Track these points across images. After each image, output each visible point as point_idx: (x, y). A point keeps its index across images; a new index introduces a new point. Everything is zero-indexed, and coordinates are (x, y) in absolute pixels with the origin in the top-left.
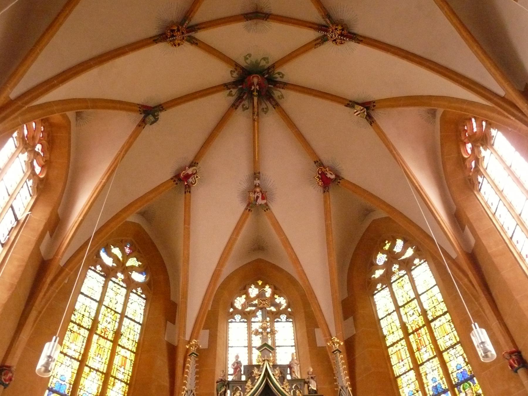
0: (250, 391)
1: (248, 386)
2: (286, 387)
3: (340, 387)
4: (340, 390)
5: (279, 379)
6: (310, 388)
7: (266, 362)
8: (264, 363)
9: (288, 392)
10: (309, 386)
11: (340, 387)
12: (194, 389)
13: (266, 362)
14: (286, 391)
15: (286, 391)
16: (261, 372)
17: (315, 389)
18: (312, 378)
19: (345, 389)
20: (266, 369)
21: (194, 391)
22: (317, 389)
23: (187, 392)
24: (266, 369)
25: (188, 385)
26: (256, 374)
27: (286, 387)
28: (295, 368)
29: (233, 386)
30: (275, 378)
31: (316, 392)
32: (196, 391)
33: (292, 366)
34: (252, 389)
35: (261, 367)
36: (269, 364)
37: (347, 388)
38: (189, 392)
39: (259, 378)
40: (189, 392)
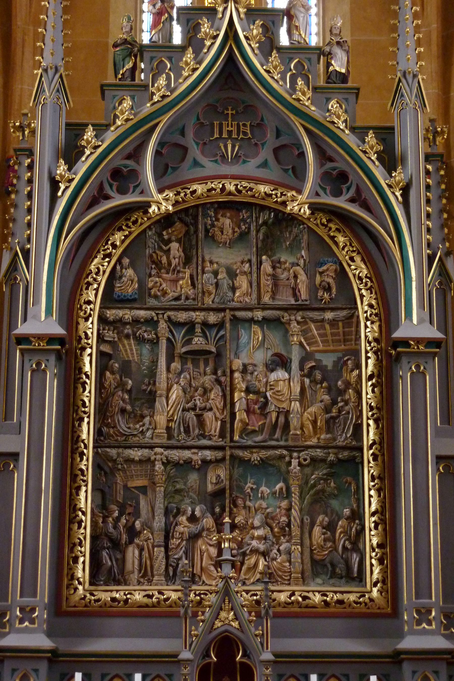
0: (190, 76)
1: (187, 64)
2: (275, 68)
3: (399, 75)
4: (400, 81)
5: (259, 48)
6: (331, 68)
7: (231, 6)
8: (225, 8)
9: (277, 81)
10: (329, 64)
11: (399, 75)
12: (60, 63)
13: (231, 6)
14: (273, 78)
15: (273, 78)
16: (219, 29)
17: (343, 71)
18: (338, 43)
19: (410, 80)
20: (231, 22)
21: (62, 70)
22: (348, 71)
23: (46, 70)
24: (231, 22)
25: (47, 54)
26: (206, 34)
27: (275, 68)
28: (301, 19)
29: (152, 59)
30: (250, 45)
31: (344, 78)
32: (66, 70)
33: (292, 13)
34: (194, 70)
35: (220, 15)
36: (237, 9)
37: (415, 76)
38: (51, 72)
39: (213, 44)
40: (51, 72)
